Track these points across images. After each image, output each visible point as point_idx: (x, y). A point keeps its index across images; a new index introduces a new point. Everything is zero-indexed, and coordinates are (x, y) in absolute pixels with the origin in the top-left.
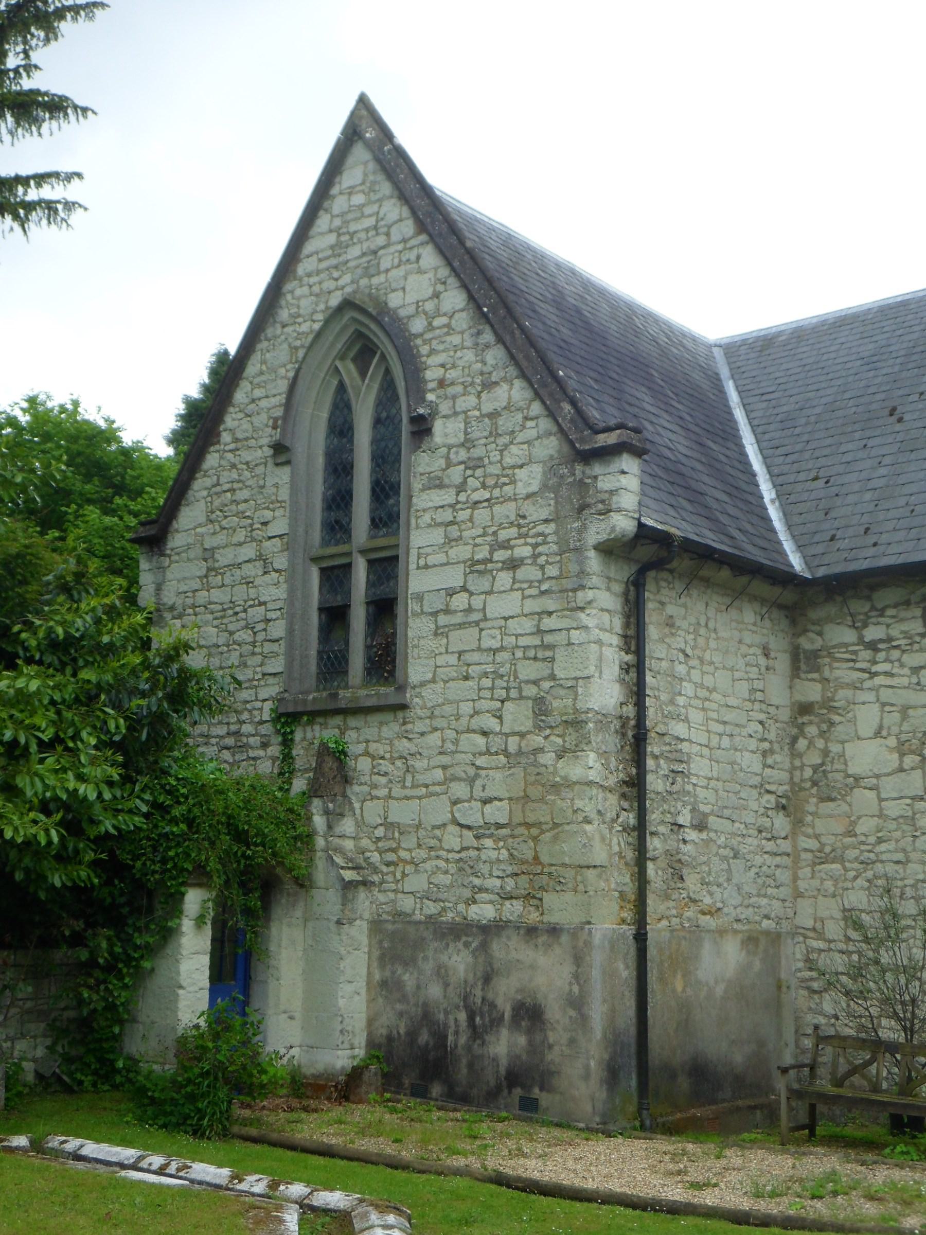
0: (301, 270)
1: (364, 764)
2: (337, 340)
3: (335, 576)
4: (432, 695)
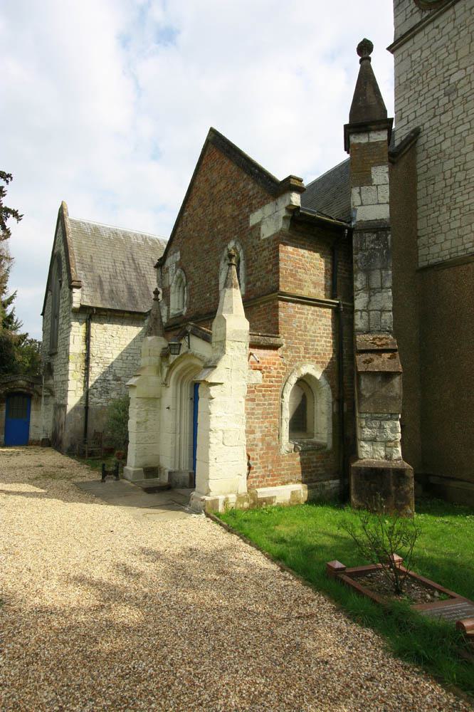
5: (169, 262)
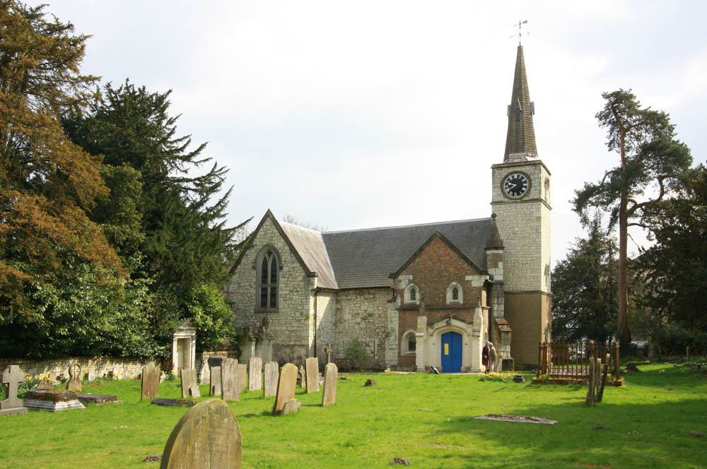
0: (258, 237)
1: (271, 321)
2: (265, 250)
3: (264, 290)
4: (283, 310)
5: (401, 277)
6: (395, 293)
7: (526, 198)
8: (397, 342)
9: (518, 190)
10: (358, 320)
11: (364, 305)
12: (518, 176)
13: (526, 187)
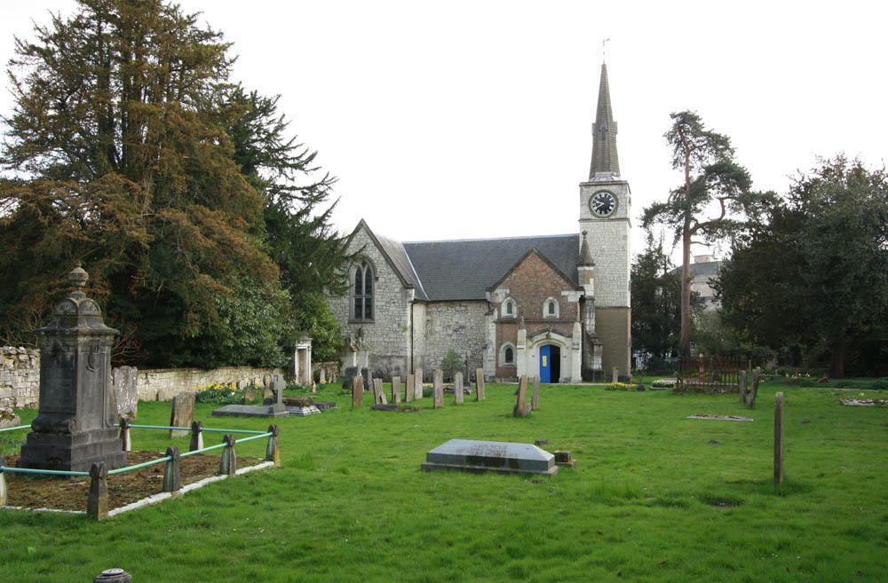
5: (497, 291)
6: (491, 306)
7: (613, 217)
8: (494, 354)
9: (605, 209)
10: (450, 332)
11: (455, 316)
12: (606, 195)
13: (612, 206)
